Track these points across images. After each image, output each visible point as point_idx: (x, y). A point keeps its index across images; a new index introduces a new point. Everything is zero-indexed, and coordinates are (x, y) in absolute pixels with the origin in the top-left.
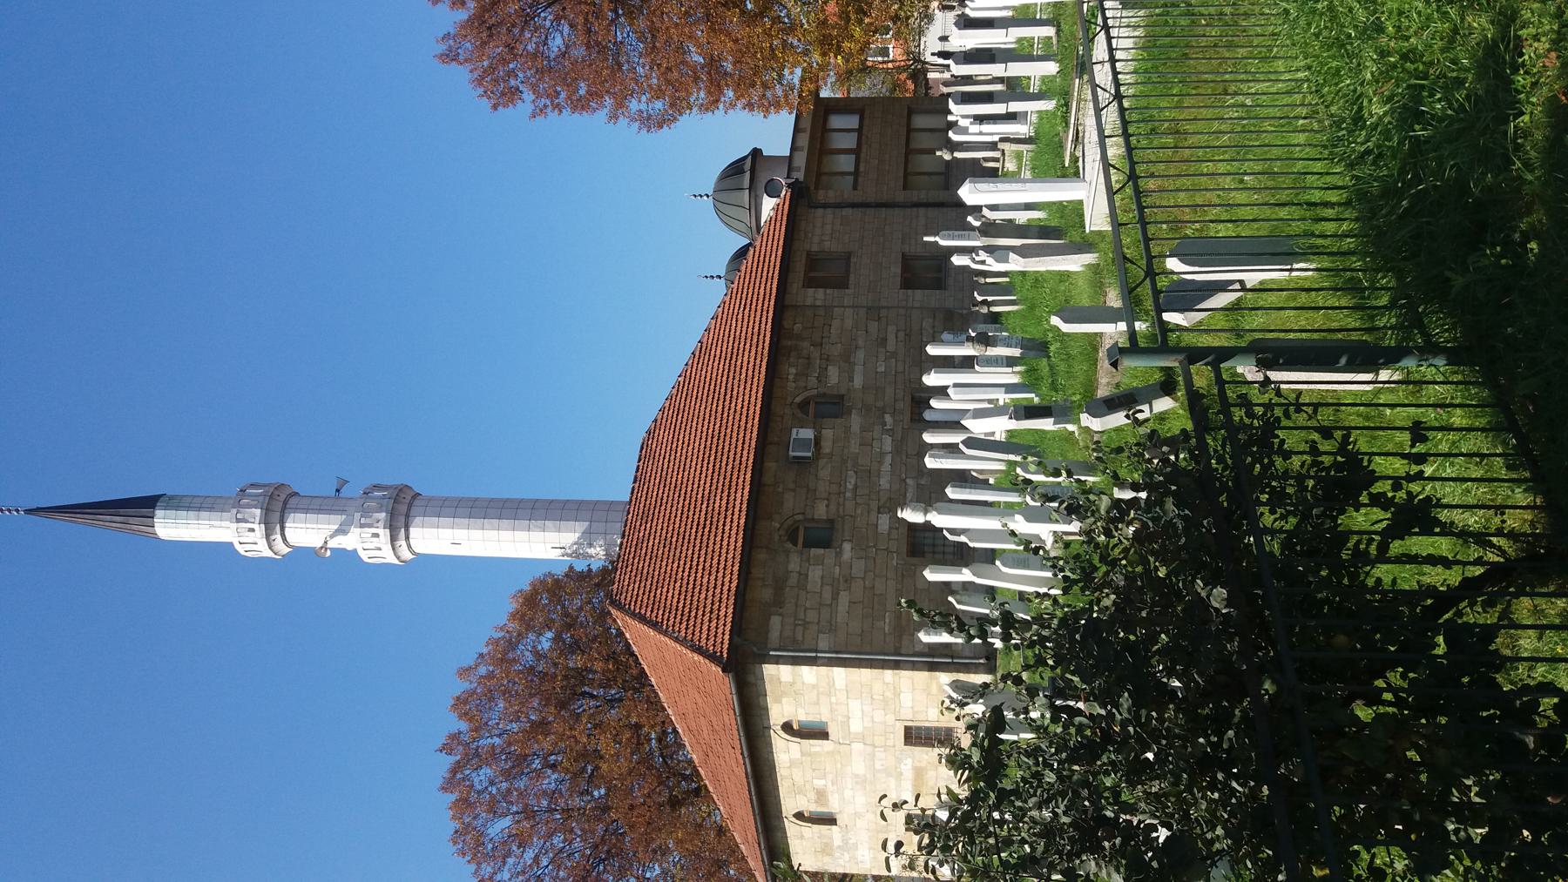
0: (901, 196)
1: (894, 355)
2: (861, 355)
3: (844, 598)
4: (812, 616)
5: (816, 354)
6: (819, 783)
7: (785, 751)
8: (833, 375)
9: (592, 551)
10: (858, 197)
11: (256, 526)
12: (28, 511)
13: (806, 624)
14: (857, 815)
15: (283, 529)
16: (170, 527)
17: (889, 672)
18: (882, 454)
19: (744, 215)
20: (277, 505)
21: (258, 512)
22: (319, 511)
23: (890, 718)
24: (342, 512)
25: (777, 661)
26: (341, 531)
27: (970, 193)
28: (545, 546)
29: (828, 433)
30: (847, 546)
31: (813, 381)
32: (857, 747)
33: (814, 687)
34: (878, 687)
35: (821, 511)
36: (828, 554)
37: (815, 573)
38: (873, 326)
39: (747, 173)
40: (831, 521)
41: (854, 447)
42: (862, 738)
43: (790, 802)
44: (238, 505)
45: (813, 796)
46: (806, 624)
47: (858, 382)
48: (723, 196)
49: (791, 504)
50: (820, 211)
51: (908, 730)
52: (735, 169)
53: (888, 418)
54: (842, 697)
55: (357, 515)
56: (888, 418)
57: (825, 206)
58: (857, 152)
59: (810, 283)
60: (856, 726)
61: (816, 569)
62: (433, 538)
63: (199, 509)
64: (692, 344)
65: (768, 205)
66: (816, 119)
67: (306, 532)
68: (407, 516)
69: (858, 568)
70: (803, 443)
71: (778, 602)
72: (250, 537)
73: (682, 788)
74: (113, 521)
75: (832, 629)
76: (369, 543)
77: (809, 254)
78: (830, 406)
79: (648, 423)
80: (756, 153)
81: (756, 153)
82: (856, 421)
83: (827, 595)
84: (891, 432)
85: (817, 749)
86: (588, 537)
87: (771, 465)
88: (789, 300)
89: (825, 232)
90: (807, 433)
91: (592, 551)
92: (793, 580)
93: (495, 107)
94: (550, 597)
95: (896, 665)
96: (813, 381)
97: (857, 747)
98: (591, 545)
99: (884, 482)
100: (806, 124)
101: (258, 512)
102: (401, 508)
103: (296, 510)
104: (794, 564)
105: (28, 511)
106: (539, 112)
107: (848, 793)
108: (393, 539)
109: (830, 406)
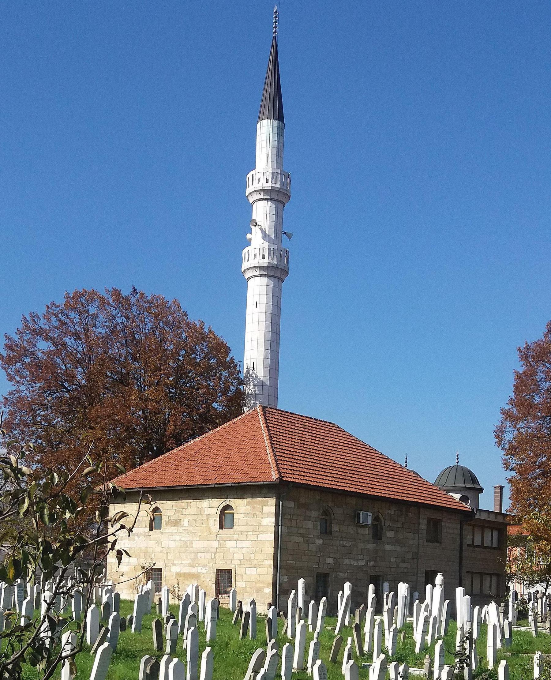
0: (464, 570)
1: (398, 567)
2: (398, 549)
3: (300, 540)
4: (294, 523)
5: (399, 525)
6: (185, 522)
7: (211, 507)
8: (390, 534)
9: (251, 386)
10: (465, 547)
11: (269, 184)
12: (275, 38)
13: (291, 520)
14: (159, 542)
15: (266, 199)
16: (265, 129)
17: (272, 563)
18: (357, 560)
19: (450, 484)
20: (278, 197)
21: (278, 186)
22: (276, 222)
23: (238, 562)
24: (276, 236)
25: (277, 506)
26: (265, 236)
27: (477, 608)
28: (253, 355)
29: (366, 531)
30: (320, 542)
31: (388, 523)
32: (215, 544)
33: (260, 524)
34: (260, 557)
35: (335, 528)
36: (317, 532)
37: (310, 525)
38: (410, 556)
39: (471, 486)
40: (330, 533)
41: (361, 545)
42: (221, 546)
43: (168, 508)
44: (283, 174)
45: (174, 518)
46: (291, 520)
47: (388, 547)
48: (460, 473)
49: (338, 512)
50: (459, 526)
51: (230, 571)
52: (474, 480)
53: (372, 563)
54: (253, 538)
55: (275, 247)
56: (372, 563)
57: (461, 529)
58: (482, 546)
59: (429, 520)
60: (229, 544)
61: (312, 526)
62: (258, 290)
63: (278, 148)
64: (386, 454)
65: (457, 496)
66: (498, 524)
67: (262, 212)
68: (273, 276)
69: (312, 547)
70: (366, 519)
71: (300, 506)
72: (263, 181)
73: (156, 444)
74: (269, 93)
75: (289, 533)
76: (257, 249)
77: (441, 521)
78: (377, 533)
79: (343, 427)
80: (481, 490)
81: (481, 490)
82: (371, 546)
83: (302, 531)
84: (366, 565)
85: (212, 522)
86: (259, 384)
87: (353, 501)
88: (422, 510)
89: (450, 528)
90: (370, 521)
91: (251, 386)
92: (308, 513)
93: (519, 350)
94: (220, 357)
95: (275, 566)
96: (388, 523)
97: (215, 544)
98: (255, 385)
99: (346, 561)
100: (492, 518)
101: (278, 186)
102: (276, 273)
103: (277, 208)
104: (315, 514)
105: (275, 38)
106: (517, 373)
107: (178, 538)
108: (261, 268)
109: (377, 533)
